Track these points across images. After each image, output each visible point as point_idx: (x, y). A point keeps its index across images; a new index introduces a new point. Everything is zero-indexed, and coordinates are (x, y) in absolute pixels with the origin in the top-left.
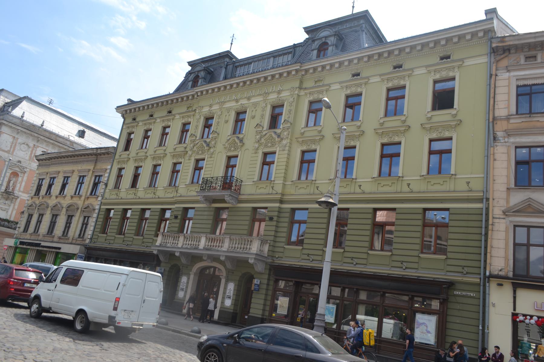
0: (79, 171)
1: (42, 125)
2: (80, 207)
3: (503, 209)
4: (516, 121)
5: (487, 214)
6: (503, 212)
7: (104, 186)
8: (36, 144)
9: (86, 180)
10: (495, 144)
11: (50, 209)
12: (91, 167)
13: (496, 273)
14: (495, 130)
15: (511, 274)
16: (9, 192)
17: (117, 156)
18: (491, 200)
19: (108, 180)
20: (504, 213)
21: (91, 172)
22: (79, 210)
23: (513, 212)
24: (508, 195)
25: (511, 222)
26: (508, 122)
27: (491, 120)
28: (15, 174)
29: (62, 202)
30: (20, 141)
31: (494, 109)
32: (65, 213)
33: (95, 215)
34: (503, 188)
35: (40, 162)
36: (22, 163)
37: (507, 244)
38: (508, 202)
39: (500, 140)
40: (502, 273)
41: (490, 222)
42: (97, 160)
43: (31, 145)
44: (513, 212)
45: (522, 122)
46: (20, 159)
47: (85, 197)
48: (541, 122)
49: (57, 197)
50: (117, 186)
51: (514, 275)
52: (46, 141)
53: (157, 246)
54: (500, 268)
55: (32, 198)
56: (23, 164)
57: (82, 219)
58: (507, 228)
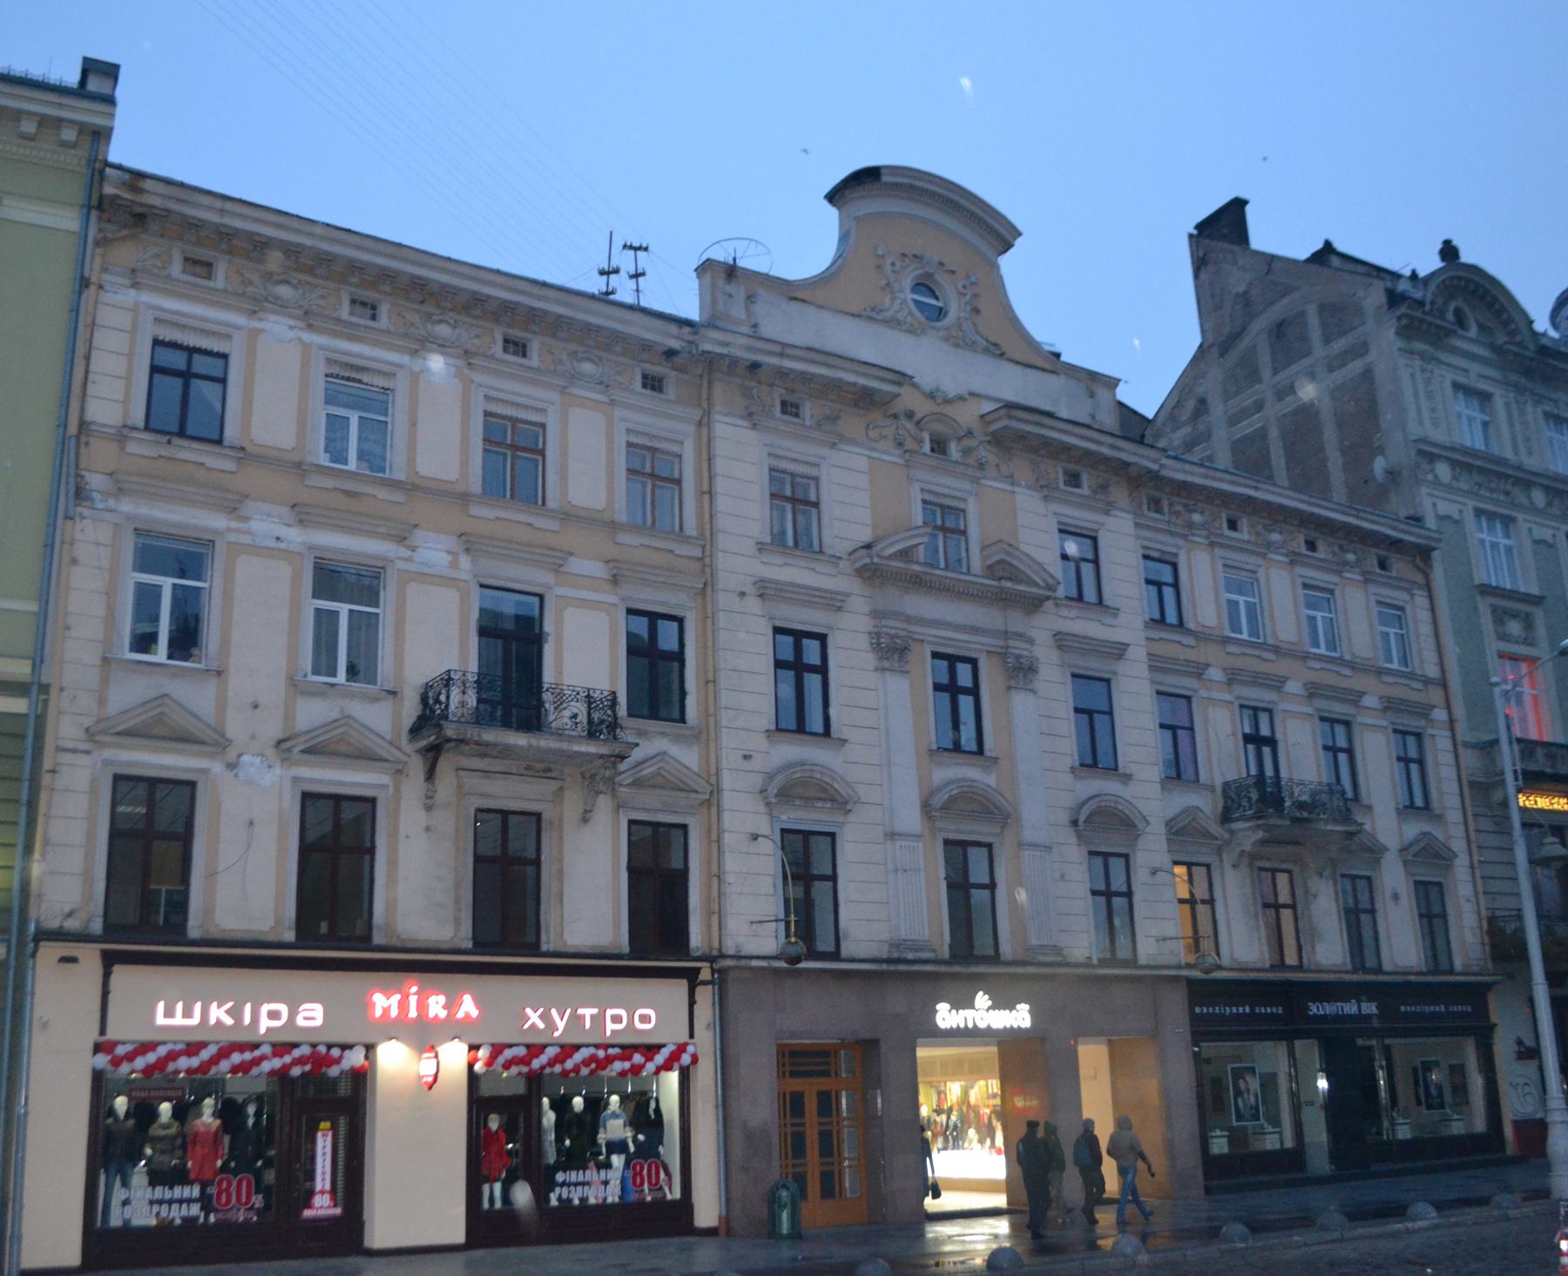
3: (88, 722)
4: (143, 447)
5: (39, 737)
6: (87, 730)
10: (79, 509)
13: (54, 924)
14: (82, 466)
15: (97, 927)
18: (54, 692)
20: (90, 734)
23: (118, 734)
24: (105, 681)
25: (106, 763)
26: (122, 448)
27: (73, 428)
31: (84, 395)
34: (92, 657)
37: (91, 834)
38: (102, 701)
39: (91, 499)
40: (72, 924)
41: (47, 764)
44: (118, 734)
45: (160, 457)
48: (209, 469)
51: (107, 926)
54: (67, 909)
58: (94, 782)
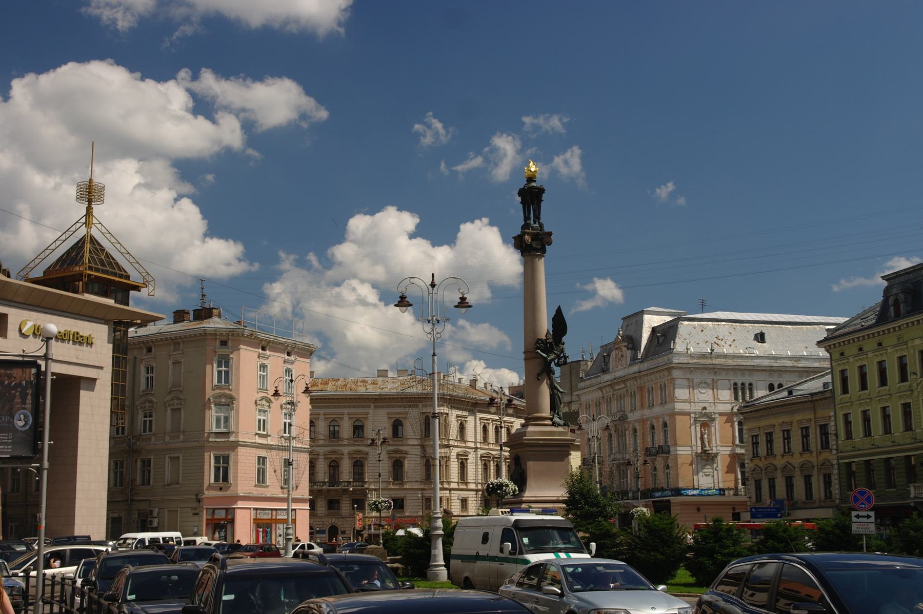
0: (799, 422)
1: (712, 350)
2: (815, 464)
7: (834, 438)
8: (715, 378)
9: (812, 431)
11: (779, 471)
12: (812, 416)
16: (706, 450)
17: (837, 402)
19: (836, 430)
21: (813, 422)
22: (816, 468)
28: (705, 425)
29: (792, 461)
30: (696, 381)
32: (800, 475)
33: (836, 472)
35: (745, 415)
36: (707, 408)
42: (814, 406)
43: (709, 381)
46: (704, 405)
47: (817, 452)
49: (783, 456)
50: (849, 436)
52: (723, 369)
53: (912, 499)
55: (752, 460)
56: (709, 410)
57: (822, 478)
